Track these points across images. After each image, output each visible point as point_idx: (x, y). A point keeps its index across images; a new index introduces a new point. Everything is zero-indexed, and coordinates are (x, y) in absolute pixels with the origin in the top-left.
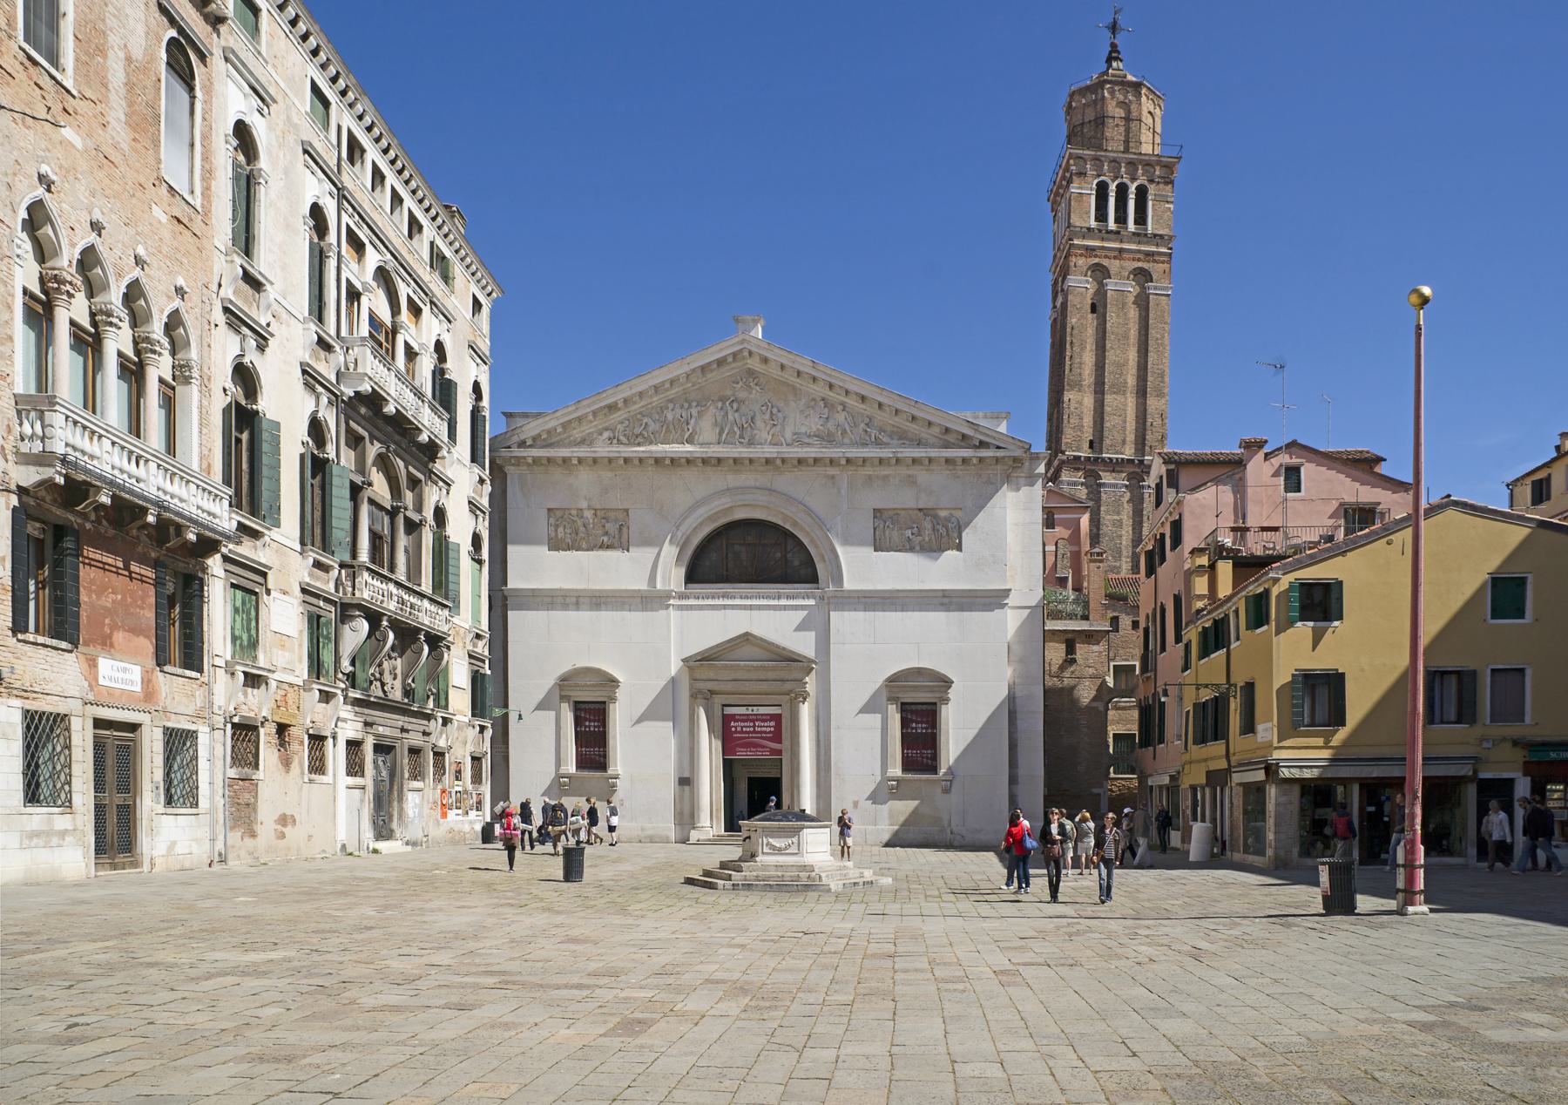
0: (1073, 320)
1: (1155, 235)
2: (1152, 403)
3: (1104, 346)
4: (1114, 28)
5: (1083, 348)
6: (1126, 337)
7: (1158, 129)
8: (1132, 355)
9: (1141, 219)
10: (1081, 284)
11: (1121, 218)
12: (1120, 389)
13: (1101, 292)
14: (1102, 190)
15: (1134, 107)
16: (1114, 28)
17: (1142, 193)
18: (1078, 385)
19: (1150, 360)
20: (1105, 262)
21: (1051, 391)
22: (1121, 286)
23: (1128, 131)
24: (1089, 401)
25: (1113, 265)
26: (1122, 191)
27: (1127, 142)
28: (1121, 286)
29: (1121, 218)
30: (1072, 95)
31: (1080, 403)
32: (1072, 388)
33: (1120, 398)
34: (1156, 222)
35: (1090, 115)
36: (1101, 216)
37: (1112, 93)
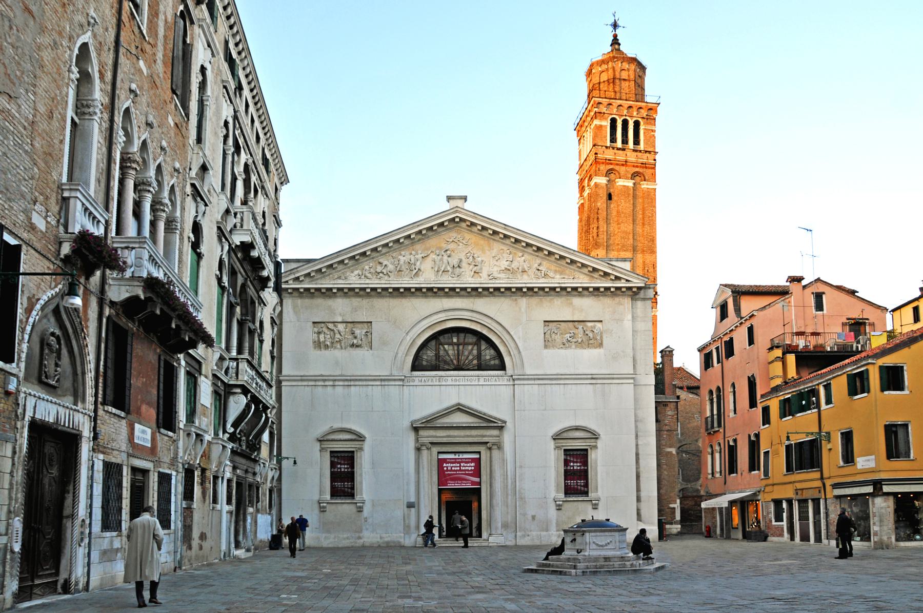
4: (615, 26)
9: (637, 142)
11: (625, 141)
14: (613, 122)
16: (615, 26)
17: (637, 124)
20: (617, 168)
26: (625, 123)
29: (625, 141)
30: (592, 65)
34: (645, 143)
36: (613, 140)
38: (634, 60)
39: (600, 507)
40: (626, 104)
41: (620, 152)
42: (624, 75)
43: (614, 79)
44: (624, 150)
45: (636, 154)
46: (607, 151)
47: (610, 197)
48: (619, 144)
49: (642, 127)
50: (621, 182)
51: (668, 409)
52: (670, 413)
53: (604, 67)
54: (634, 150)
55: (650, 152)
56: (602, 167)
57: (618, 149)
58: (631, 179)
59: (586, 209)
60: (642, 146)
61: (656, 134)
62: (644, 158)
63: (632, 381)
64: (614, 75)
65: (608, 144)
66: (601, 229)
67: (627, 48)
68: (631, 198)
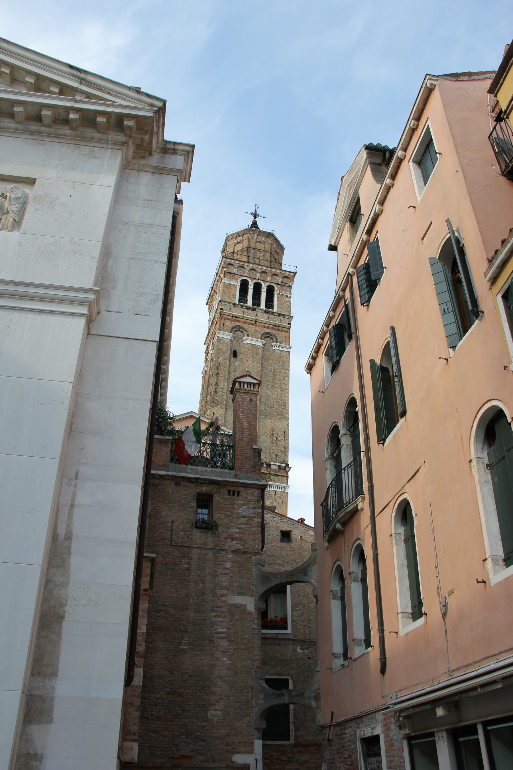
1: (279, 315)
4: (255, 215)
14: (244, 285)
16: (255, 215)
17: (270, 291)
20: (245, 326)
26: (257, 288)
38: (270, 235)
40: (259, 269)
41: (250, 311)
42: (260, 246)
43: (249, 247)
44: (254, 310)
45: (268, 315)
47: (235, 354)
48: (250, 303)
49: (276, 292)
50: (248, 341)
51: (239, 501)
52: (243, 511)
53: (239, 239)
54: (265, 312)
55: (284, 316)
56: (228, 323)
57: (248, 308)
58: (261, 338)
59: (208, 372)
60: (275, 310)
61: (292, 301)
62: (277, 321)
63: (84, 310)
64: (249, 244)
66: (221, 386)
67: (263, 226)
68: (260, 357)
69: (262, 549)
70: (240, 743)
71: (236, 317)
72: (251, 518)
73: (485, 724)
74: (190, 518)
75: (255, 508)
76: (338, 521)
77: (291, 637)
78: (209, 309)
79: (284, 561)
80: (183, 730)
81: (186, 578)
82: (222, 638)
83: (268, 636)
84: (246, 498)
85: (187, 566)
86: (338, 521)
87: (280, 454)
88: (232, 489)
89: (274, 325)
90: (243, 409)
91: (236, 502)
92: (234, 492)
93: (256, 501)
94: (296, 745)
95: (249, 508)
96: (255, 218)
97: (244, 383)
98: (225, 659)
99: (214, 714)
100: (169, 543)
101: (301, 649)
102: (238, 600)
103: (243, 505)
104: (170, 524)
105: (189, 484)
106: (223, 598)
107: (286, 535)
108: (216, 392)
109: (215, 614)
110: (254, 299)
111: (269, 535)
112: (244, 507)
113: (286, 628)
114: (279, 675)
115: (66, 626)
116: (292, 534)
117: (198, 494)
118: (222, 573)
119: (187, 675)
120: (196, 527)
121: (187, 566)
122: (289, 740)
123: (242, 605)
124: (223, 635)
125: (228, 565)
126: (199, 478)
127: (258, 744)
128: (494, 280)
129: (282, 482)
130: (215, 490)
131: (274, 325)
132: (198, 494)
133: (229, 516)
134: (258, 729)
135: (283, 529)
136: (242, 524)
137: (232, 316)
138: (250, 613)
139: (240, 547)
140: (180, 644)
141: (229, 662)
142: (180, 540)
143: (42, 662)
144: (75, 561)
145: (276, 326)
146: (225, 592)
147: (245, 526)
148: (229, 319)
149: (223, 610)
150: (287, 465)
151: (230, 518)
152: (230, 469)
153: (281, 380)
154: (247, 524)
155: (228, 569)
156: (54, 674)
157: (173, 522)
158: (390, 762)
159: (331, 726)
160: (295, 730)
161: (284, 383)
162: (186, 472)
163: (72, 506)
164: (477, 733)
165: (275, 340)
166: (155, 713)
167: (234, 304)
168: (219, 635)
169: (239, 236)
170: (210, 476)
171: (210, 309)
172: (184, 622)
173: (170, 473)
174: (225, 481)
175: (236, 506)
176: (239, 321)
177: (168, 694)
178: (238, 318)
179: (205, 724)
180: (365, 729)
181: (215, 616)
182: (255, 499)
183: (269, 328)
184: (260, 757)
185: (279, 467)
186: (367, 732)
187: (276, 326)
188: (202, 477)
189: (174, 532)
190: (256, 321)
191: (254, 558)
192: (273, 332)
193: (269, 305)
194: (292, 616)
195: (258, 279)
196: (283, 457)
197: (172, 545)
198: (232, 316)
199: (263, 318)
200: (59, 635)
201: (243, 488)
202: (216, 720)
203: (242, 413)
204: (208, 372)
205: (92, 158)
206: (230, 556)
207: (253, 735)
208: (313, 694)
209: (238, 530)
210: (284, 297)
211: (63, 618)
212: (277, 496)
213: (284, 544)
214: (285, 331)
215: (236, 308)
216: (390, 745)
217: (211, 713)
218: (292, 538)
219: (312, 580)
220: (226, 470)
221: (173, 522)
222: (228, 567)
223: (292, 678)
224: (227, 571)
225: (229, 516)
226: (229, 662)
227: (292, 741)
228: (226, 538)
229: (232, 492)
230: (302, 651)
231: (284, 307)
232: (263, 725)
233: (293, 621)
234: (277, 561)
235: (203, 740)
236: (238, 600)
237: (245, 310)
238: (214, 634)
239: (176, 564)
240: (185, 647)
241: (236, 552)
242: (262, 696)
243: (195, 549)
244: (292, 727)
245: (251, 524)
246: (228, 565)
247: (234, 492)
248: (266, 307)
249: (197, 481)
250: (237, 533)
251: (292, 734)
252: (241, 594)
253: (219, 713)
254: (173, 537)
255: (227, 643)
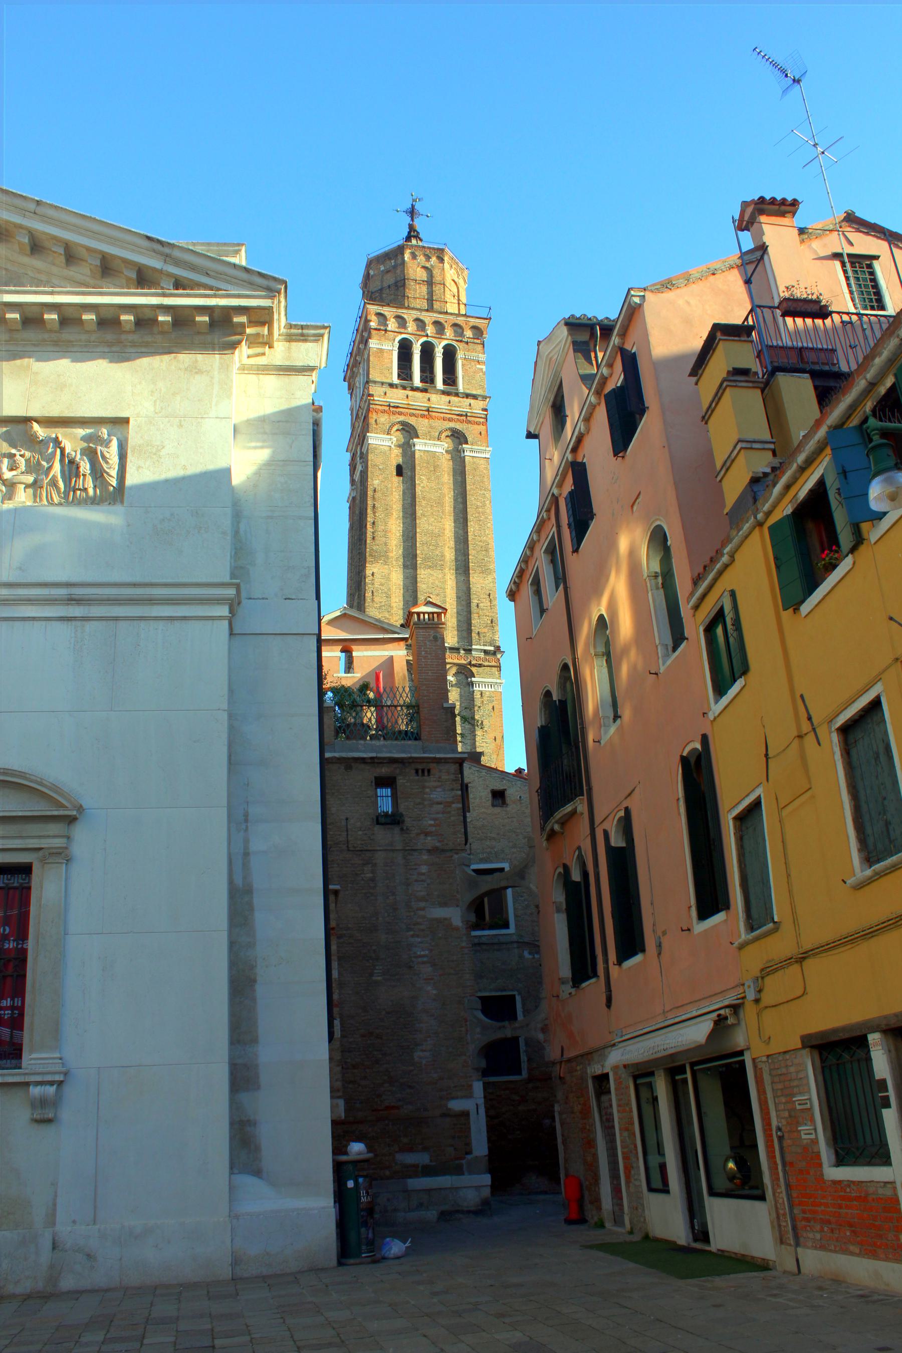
0: (374, 482)
1: (467, 396)
2: (476, 580)
3: (414, 514)
4: (412, 212)
5: (388, 514)
6: (440, 503)
7: (463, 299)
8: (449, 526)
10: (383, 443)
12: (436, 564)
13: (407, 448)
15: (436, 272)
16: (412, 212)
18: (384, 557)
19: (471, 530)
20: (412, 421)
21: (350, 579)
22: (431, 447)
23: (431, 293)
24: (397, 577)
25: (421, 425)
27: (430, 300)
28: (431, 447)
31: (388, 578)
32: (376, 559)
33: (437, 574)
34: (467, 382)
35: (390, 279)
37: (414, 256)
39: (66, 1114)
44: (425, 391)
45: (447, 398)
46: (390, 391)
48: (417, 381)
49: (460, 355)
54: (444, 393)
58: (439, 439)
59: (357, 501)
60: (461, 387)
65: (396, 381)
69: (466, 844)
70: (455, 1087)
71: (394, 407)
72: (448, 804)
73: (692, 1065)
74: (369, 811)
75: (453, 790)
76: (557, 822)
77: (515, 938)
78: (349, 389)
79: (498, 834)
80: (386, 1078)
81: (371, 891)
82: (423, 963)
83: (484, 940)
84: (440, 778)
85: (371, 875)
86: (557, 822)
87: (486, 630)
88: (420, 767)
89: (458, 415)
90: (426, 652)
91: (427, 784)
92: (423, 771)
93: (454, 780)
94: (530, 1080)
95: (444, 790)
96: (412, 220)
97: (424, 613)
98: (429, 988)
99: (421, 1055)
100: (344, 847)
101: (530, 953)
102: (439, 913)
103: (436, 787)
104: (344, 823)
105: (362, 766)
106: (421, 913)
107: (499, 796)
108: (374, 538)
109: (412, 933)
110: (422, 370)
111: (475, 798)
112: (438, 790)
113: (506, 926)
114: (502, 991)
115: (260, 990)
116: (507, 793)
117: (376, 778)
118: (416, 881)
119: (384, 1012)
120: (378, 823)
121: (371, 875)
122: (520, 1074)
123: (445, 919)
124: (425, 959)
125: (424, 869)
126: (376, 758)
127: (478, 1088)
128: (696, 607)
129: (491, 675)
130: (398, 771)
131: (458, 415)
132: (376, 778)
133: (420, 804)
134: (477, 1069)
135: (495, 788)
136: (438, 813)
137: (389, 406)
138: (457, 929)
139: (438, 844)
140: (371, 975)
141: (434, 992)
142: (359, 842)
143: (242, 1030)
144: (259, 917)
145: (461, 415)
146: (422, 904)
147: (441, 815)
148: (384, 412)
149: (422, 927)
150: (498, 648)
151: (421, 806)
152: (416, 739)
153: (477, 507)
154: (443, 813)
155: (423, 874)
156: (255, 1041)
157: (347, 819)
158: (619, 1100)
159: (561, 1062)
160: (528, 1060)
161: (483, 513)
162: (358, 750)
163: (246, 854)
164: (685, 1073)
165: (462, 440)
166: (349, 1060)
167: (391, 385)
168: (420, 960)
169: (390, 259)
170: (390, 752)
171: (351, 388)
172: (374, 948)
173: (337, 755)
174: (411, 758)
175: (427, 790)
176: (400, 414)
177: (363, 1036)
178: (397, 407)
179: (412, 1068)
180: (596, 1066)
181: (412, 936)
182: (452, 777)
183: (450, 420)
184: (481, 1101)
185: (486, 652)
186: (597, 1070)
187: (461, 415)
188: (379, 755)
189: (350, 833)
190: (428, 411)
191: (456, 856)
192: (458, 426)
193: (449, 379)
194: (515, 909)
195: (427, 336)
196: (489, 635)
197: (349, 850)
198: (389, 406)
199: (439, 402)
200: (254, 1000)
201: (435, 765)
202: (424, 1062)
203: (425, 657)
204: (357, 501)
205: (196, 373)
206: (425, 857)
207: (471, 1077)
208: (539, 1026)
209: (432, 822)
210: (473, 363)
211: (255, 981)
212: (485, 698)
213: (497, 810)
214: (478, 424)
215: (395, 390)
216: (619, 1083)
217: (417, 1054)
218: (508, 800)
219: (531, 885)
220: (410, 742)
221: (347, 819)
222: (423, 871)
223: (520, 994)
224: (423, 877)
225: (420, 804)
226: (434, 992)
227: (525, 1074)
228: (418, 834)
229: (420, 772)
230: (531, 957)
231: (473, 382)
232: (483, 1064)
233: (516, 916)
234: (489, 835)
235: (410, 1087)
236: (439, 913)
237: (410, 393)
238: (413, 959)
239: (356, 874)
240: (379, 978)
241: (433, 851)
242: (478, 1030)
243: (380, 853)
244: (524, 1057)
245: (449, 812)
246: (424, 869)
247: (423, 771)
248: (445, 383)
249: (373, 761)
250: (431, 825)
251: (524, 1066)
252: (444, 904)
253: (427, 1054)
254: (350, 839)
255: (430, 969)
